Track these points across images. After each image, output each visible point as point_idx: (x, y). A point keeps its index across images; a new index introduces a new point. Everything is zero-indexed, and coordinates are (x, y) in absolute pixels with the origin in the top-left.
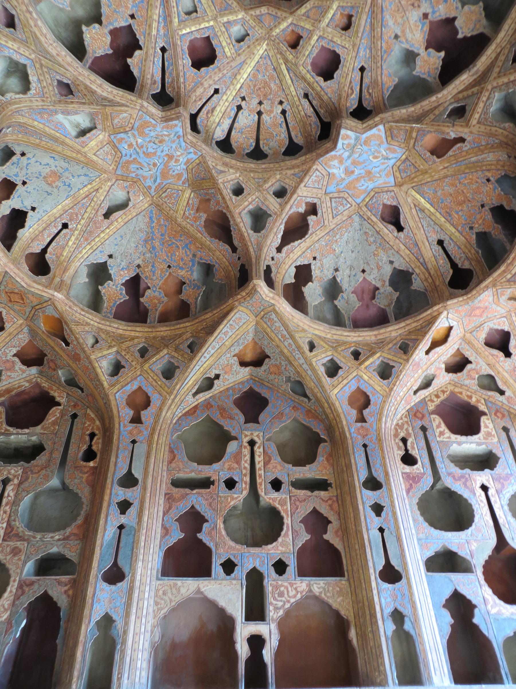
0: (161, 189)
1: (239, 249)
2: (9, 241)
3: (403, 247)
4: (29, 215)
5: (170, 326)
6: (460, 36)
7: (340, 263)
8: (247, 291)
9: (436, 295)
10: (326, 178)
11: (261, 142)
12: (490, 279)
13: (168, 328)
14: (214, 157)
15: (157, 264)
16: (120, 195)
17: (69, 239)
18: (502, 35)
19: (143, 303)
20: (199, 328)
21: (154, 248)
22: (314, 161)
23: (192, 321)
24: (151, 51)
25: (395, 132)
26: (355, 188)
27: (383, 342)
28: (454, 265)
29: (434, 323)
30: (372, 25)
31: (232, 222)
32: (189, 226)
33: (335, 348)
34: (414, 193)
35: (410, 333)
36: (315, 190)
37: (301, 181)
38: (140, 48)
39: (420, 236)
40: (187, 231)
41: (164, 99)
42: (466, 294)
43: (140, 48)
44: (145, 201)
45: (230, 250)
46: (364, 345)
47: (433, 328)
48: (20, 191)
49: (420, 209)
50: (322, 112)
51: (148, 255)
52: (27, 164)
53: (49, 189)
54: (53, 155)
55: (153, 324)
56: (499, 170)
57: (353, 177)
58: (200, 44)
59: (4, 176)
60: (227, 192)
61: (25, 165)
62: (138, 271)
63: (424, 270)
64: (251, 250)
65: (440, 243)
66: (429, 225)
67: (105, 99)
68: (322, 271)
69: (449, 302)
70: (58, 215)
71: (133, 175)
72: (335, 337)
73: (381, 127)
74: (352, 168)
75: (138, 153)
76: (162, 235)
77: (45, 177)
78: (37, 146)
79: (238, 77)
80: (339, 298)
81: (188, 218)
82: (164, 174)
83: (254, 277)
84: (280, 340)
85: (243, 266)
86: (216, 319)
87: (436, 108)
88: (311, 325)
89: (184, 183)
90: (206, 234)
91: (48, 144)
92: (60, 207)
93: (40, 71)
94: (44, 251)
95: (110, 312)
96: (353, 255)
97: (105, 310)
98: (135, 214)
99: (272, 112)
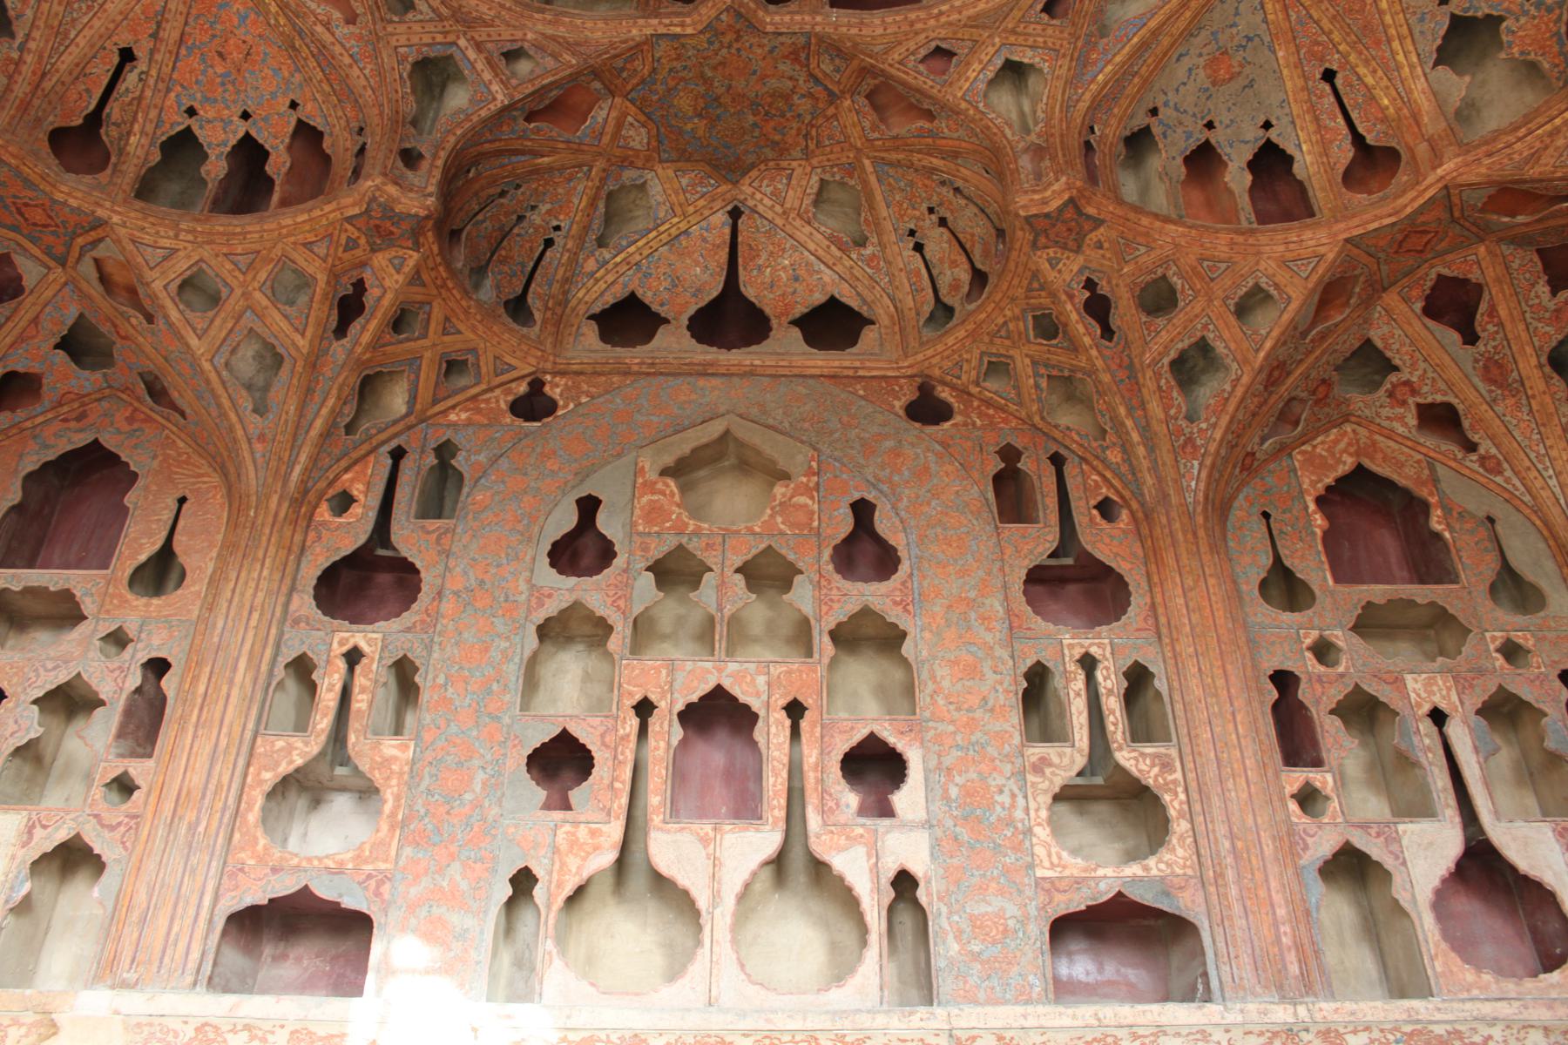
4: (1274, 139)
17: (1359, 78)
52: (1176, 109)
53: (1241, 81)
54: (1175, 56)
59: (1180, 160)
61: (1175, 114)
70: (1300, 83)
77: (1214, 84)
92: (1285, 72)
93: (1021, 40)
94: (1358, 139)
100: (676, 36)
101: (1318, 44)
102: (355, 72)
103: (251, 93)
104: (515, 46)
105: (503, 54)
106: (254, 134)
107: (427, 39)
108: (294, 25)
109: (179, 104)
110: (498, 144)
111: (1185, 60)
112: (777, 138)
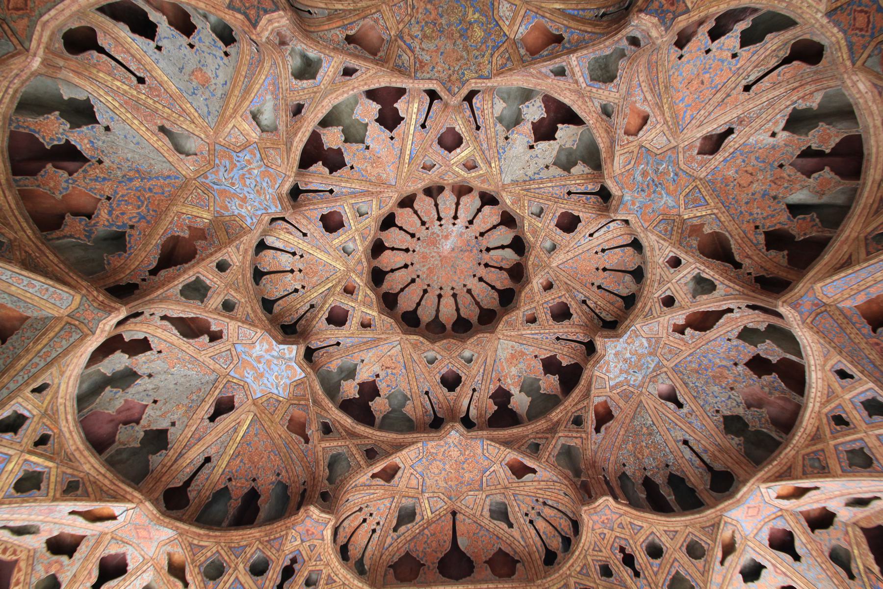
0: (207, 189)
1: (156, 278)
2: (113, 12)
3: (193, 429)
5: (18, 208)
6: (370, 403)
7: (160, 376)
8: (106, 301)
9: (151, 486)
10: (250, 342)
11: (268, 276)
12: (186, 527)
13: (13, 206)
14: (251, 240)
15: (109, 184)
16: (191, 145)
17: (124, 83)
18: (379, 433)
19: (44, 167)
20: (27, 249)
21: (131, 180)
22: (264, 328)
23: (37, 238)
24: (329, 182)
25: (302, 387)
26: (245, 368)
27: (71, 460)
28: (188, 483)
29: (117, 502)
30: (367, 342)
31: (186, 266)
32: (170, 219)
33: (45, 414)
34: (250, 418)
35: (94, 483)
36: (236, 335)
37: (243, 322)
38: (331, 173)
39: (209, 439)
40: (163, 217)
41: (295, 193)
42: (163, 514)
43: (331, 173)
44: (189, 172)
45: (151, 267)
46: (59, 443)
47: (109, 504)
48: (180, 39)
49: (236, 429)
50: (303, 322)
51: (119, 173)
53: (188, 70)
55: (14, 184)
56: (289, 479)
57: (255, 364)
58: (337, 218)
59: (199, 27)
60: (219, 257)
62: (94, 160)
63: (174, 458)
64: (159, 293)
65: (208, 460)
66: (222, 443)
67: (292, 144)
68: (145, 363)
69: (147, 504)
70: (154, 74)
71: (217, 162)
72: (61, 408)
73: (303, 375)
74: (262, 360)
75: (242, 169)
76: (150, 190)
77: (201, 70)
78: (237, 70)
79: (318, 251)
80: (115, 390)
81: (179, 218)
82: (223, 192)
83: (128, 307)
84: (39, 352)
85: (135, 286)
86: (50, 269)
87: (325, 410)
88: (73, 378)
89: (218, 212)
90: (164, 239)
91: (240, 83)
92: (166, 79)
93: (311, 90)
94: (101, 50)
95: (19, 126)
96: (172, 386)
97: (21, 119)
98: (171, 160)
99: (295, 281)
100: (480, 77)
101: (157, 96)
102: (641, 80)
103: (698, 63)
104: (558, 78)
105: (565, 75)
106: (710, 41)
107: (601, 91)
108: (661, 99)
109: (738, 61)
110: (583, 28)
111: (223, 82)
112: (429, 6)
